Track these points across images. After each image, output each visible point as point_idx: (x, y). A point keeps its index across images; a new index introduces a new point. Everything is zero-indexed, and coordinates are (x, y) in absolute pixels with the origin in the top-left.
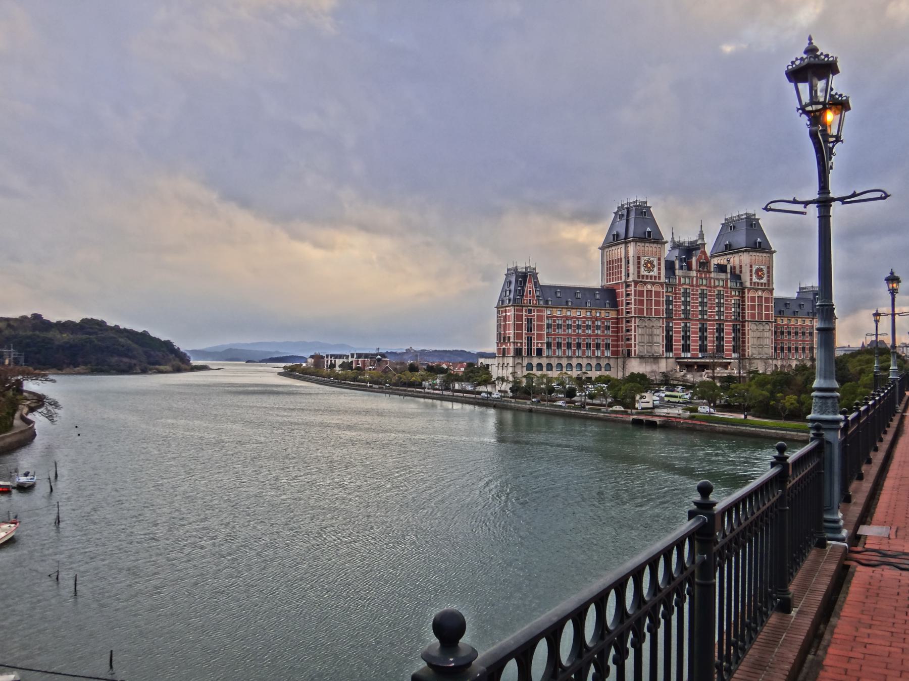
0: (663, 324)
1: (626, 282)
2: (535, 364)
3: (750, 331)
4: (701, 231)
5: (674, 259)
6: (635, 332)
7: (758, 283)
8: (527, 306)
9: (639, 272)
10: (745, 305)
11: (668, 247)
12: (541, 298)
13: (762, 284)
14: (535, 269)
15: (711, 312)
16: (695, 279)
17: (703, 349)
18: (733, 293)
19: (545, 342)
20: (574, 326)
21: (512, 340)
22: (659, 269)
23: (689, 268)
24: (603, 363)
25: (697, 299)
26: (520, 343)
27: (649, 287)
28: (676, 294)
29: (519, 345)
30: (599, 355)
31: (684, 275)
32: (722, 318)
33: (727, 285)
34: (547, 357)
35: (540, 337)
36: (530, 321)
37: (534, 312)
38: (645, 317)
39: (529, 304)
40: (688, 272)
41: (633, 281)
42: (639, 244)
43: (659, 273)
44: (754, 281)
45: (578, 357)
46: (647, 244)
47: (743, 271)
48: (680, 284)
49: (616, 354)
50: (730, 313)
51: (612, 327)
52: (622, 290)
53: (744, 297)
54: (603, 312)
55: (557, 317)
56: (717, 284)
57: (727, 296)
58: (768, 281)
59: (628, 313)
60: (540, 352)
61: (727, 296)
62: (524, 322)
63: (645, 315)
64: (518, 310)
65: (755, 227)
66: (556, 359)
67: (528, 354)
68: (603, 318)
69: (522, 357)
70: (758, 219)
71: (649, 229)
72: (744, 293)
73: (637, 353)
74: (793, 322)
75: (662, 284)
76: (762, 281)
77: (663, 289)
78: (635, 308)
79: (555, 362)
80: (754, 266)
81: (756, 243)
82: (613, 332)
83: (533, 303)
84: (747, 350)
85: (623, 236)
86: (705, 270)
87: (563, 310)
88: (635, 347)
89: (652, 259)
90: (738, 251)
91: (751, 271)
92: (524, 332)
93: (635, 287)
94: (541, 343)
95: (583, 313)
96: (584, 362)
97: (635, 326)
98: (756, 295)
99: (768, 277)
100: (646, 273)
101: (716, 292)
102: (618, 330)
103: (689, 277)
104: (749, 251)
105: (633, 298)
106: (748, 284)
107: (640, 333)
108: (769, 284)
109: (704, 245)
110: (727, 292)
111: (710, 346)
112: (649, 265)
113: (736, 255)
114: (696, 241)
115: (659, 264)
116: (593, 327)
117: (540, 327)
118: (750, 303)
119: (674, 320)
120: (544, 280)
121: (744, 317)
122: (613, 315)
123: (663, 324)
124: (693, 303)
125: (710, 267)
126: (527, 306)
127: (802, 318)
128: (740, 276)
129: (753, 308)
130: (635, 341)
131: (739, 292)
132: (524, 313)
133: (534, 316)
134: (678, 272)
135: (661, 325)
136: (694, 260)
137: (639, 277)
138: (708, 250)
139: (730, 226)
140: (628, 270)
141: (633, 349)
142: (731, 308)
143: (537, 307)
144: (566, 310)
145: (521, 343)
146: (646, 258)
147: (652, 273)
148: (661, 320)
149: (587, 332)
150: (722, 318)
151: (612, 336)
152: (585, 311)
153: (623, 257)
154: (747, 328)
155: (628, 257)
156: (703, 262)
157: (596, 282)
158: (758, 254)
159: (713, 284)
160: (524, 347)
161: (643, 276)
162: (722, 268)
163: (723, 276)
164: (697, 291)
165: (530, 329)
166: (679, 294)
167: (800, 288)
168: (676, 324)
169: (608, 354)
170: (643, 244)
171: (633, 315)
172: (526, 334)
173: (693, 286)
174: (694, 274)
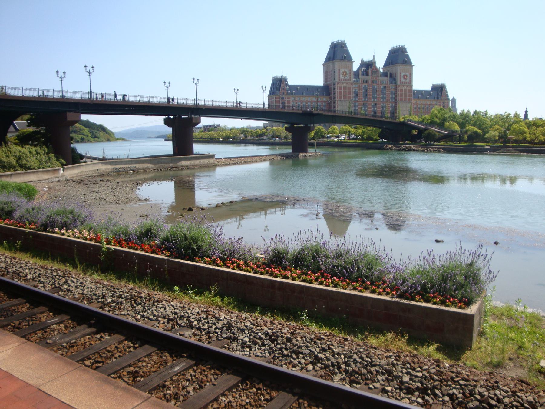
4: (374, 56)
7: (404, 83)
14: (286, 77)
22: (350, 75)
23: (367, 75)
43: (350, 78)
52: (332, 87)
75: (352, 84)
76: (407, 81)
89: (346, 70)
100: (343, 78)
112: (345, 74)
115: (350, 73)
120: (291, 82)
121: (396, 100)
134: (361, 77)
146: (343, 70)
147: (346, 78)
150: (385, 100)
163: (385, 78)
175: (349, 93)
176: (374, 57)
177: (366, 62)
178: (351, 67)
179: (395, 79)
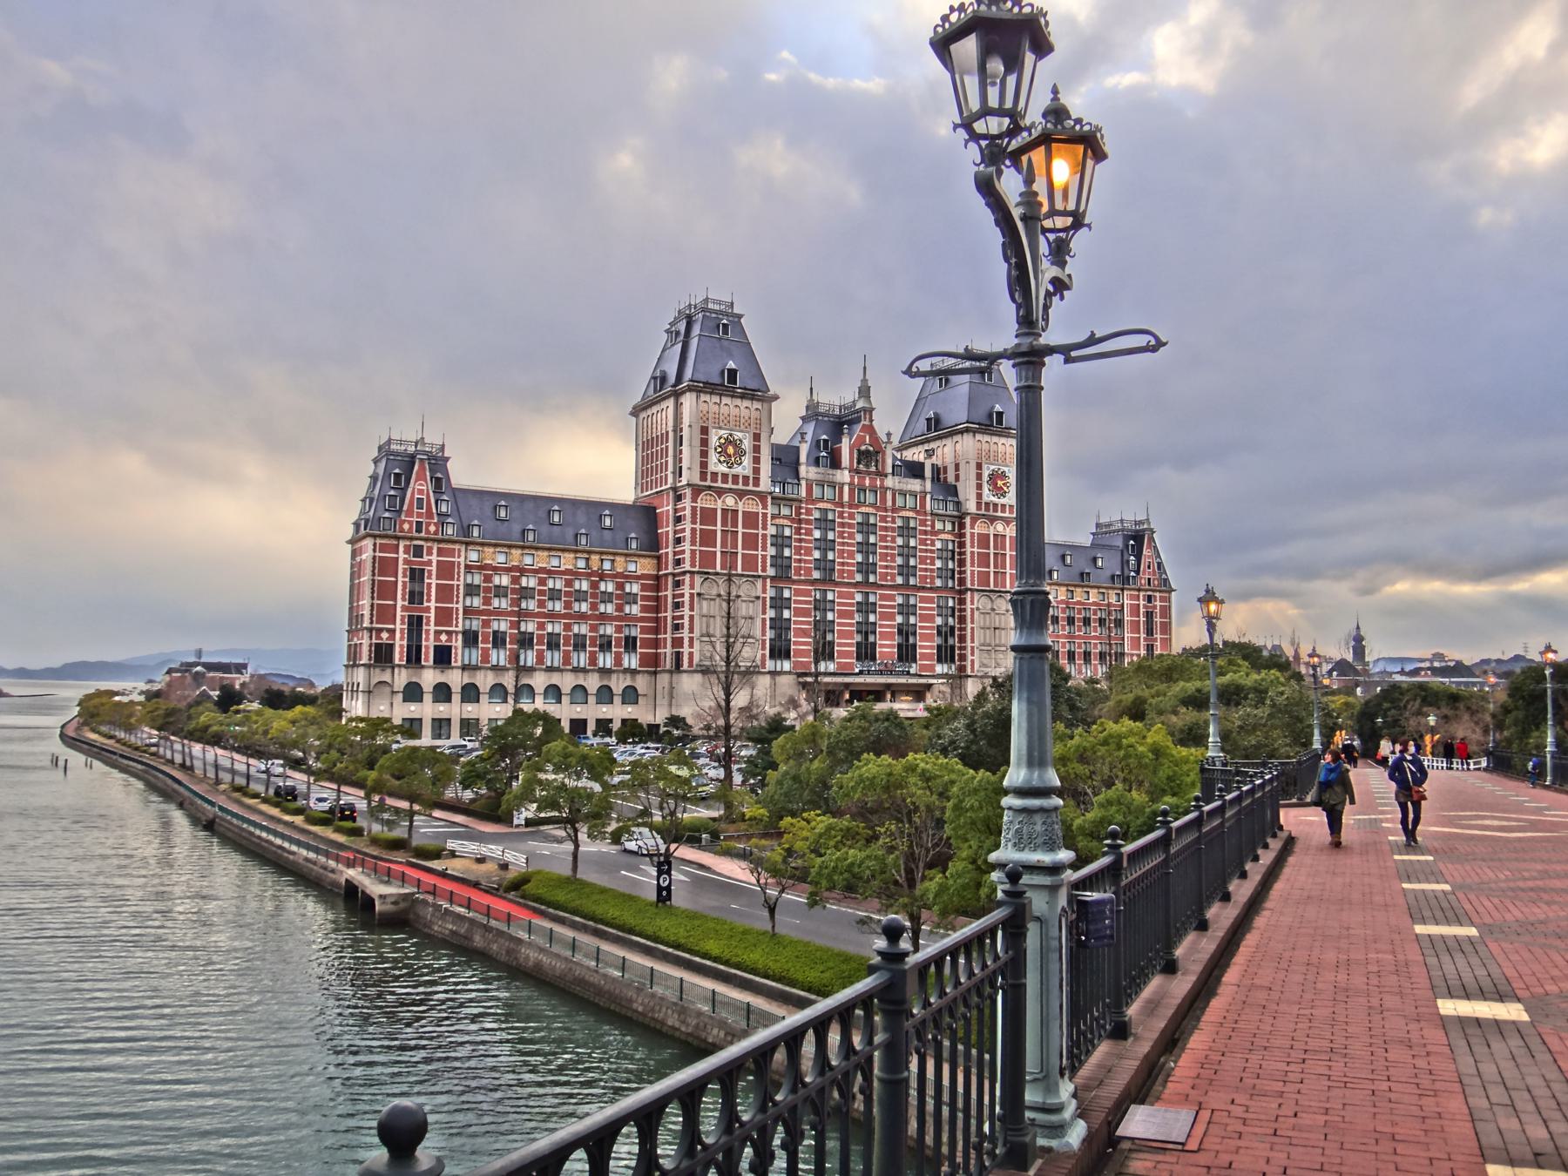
0: (764, 591)
1: (675, 489)
2: (456, 688)
3: (976, 613)
4: (865, 380)
6: (692, 609)
7: (995, 505)
8: (412, 539)
9: (704, 465)
10: (964, 553)
12: (450, 520)
13: (1003, 506)
15: (887, 567)
16: (846, 488)
17: (866, 652)
18: (939, 526)
19: (460, 628)
20: (541, 593)
21: (366, 624)
22: (757, 460)
23: (835, 463)
24: (618, 684)
25: (851, 536)
26: (388, 630)
27: (730, 501)
28: (800, 521)
29: (385, 635)
30: (608, 666)
31: (819, 477)
32: (912, 581)
33: (923, 505)
34: (464, 668)
35: (444, 616)
36: (416, 575)
37: (430, 553)
38: (717, 574)
39: (415, 534)
40: (831, 471)
41: (688, 485)
42: (704, 397)
43: (756, 471)
45: (550, 669)
46: (726, 400)
47: (962, 477)
48: (810, 499)
49: (652, 663)
50: (932, 570)
51: (644, 598)
52: (666, 508)
53: (962, 535)
54: (618, 559)
55: (495, 569)
56: (899, 502)
57: (925, 533)
59: (678, 562)
60: (443, 657)
61: (925, 533)
62: (400, 579)
63: (718, 569)
64: (383, 548)
66: (490, 675)
67: (408, 661)
68: (618, 575)
69: (393, 668)
71: (731, 365)
72: (962, 526)
73: (696, 659)
74: (1079, 595)
75: (762, 497)
76: (1003, 501)
77: (765, 507)
78: (693, 552)
79: (485, 681)
80: (985, 466)
81: (990, 416)
82: (644, 609)
83: (428, 532)
84: (970, 658)
85: (672, 379)
86: (873, 469)
87: (514, 551)
88: (691, 646)
89: (738, 435)
91: (979, 476)
92: (400, 603)
93: (694, 500)
94: (449, 633)
95: (566, 562)
96: (567, 682)
97: (692, 595)
98: (992, 532)
100: (723, 468)
101: (899, 523)
102: (657, 605)
103: (832, 485)
104: (975, 432)
105: (687, 525)
106: (971, 507)
107: (705, 611)
109: (871, 410)
110: (923, 523)
111: (887, 648)
112: (731, 450)
113: (949, 442)
115: (757, 449)
116: (594, 596)
117: (445, 593)
118: (976, 550)
119: (794, 582)
121: (962, 581)
122: (644, 566)
123: (764, 591)
124: (843, 544)
125: (884, 461)
126: (412, 539)
127: (1098, 587)
128: (955, 487)
129: (984, 560)
130: (691, 630)
131: (953, 523)
132: (402, 556)
133: (429, 563)
134: (803, 470)
135: (759, 593)
136: (845, 445)
137: (703, 476)
140: (681, 461)
141: (686, 650)
142: (933, 559)
143: (440, 541)
144: (519, 551)
145: (392, 632)
147: (737, 470)
148: (759, 583)
149: (576, 607)
150: (912, 581)
151: (642, 619)
152: (572, 555)
153: (670, 429)
154: (969, 606)
155: (681, 430)
156: (868, 451)
157: (624, 490)
158: (995, 439)
159: (889, 503)
160: (398, 642)
161: (714, 475)
163: (914, 485)
164: (851, 516)
165: (415, 597)
166: (808, 522)
167: (1098, 525)
168: (798, 592)
169: (631, 661)
170: (716, 399)
171: (687, 566)
172: (404, 608)
173: (843, 506)
174: (844, 476)
175: (751, 542)
179: (953, 491)
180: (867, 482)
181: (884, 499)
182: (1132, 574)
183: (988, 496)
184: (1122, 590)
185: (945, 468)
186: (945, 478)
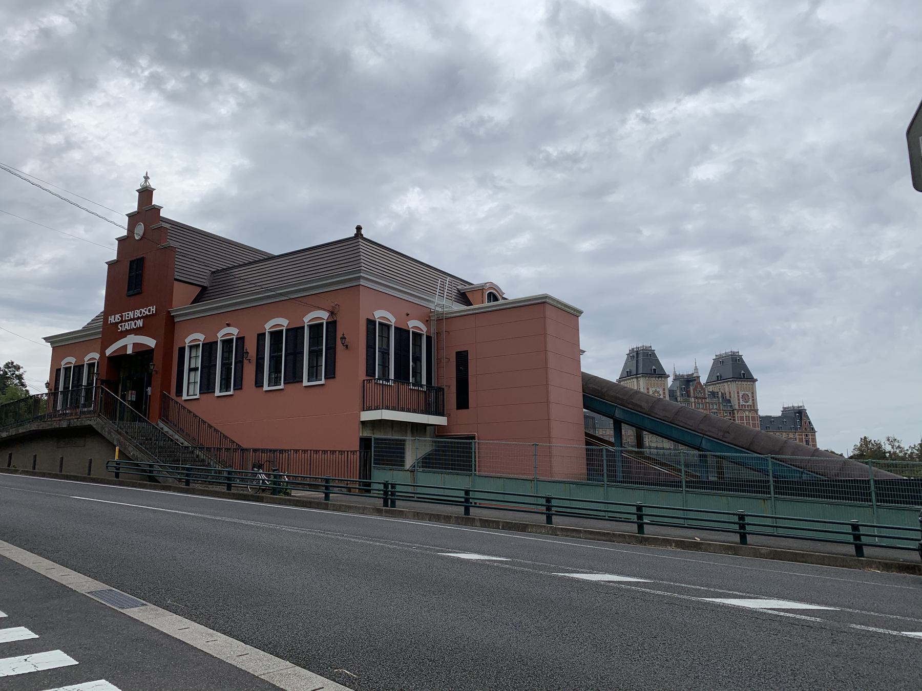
4: (696, 367)
5: (675, 389)
7: (745, 406)
11: (670, 381)
13: (748, 406)
16: (693, 403)
44: (741, 404)
47: (732, 396)
53: (734, 417)
58: (753, 403)
65: (739, 362)
70: (741, 356)
72: (734, 414)
76: (748, 404)
80: (740, 392)
89: (658, 390)
90: (726, 380)
91: (738, 396)
99: (753, 400)
108: (754, 406)
114: (693, 374)
127: (786, 432)
128: (730, 400)
138: (703, 380)
139: (720, 361)
146: (654, 389)
158: (743, 383)
162: (713, 394)
163: (715, 400)
176: (696, 369)
177: (683, 376)
178: (666, 383)
179: (729, 401)
180: (700, 401)
181: (706, 406)
182: (799, 426)
183: (742, 403)
184: (795, 432)
185: (725, 393)
186: (726, 397)
